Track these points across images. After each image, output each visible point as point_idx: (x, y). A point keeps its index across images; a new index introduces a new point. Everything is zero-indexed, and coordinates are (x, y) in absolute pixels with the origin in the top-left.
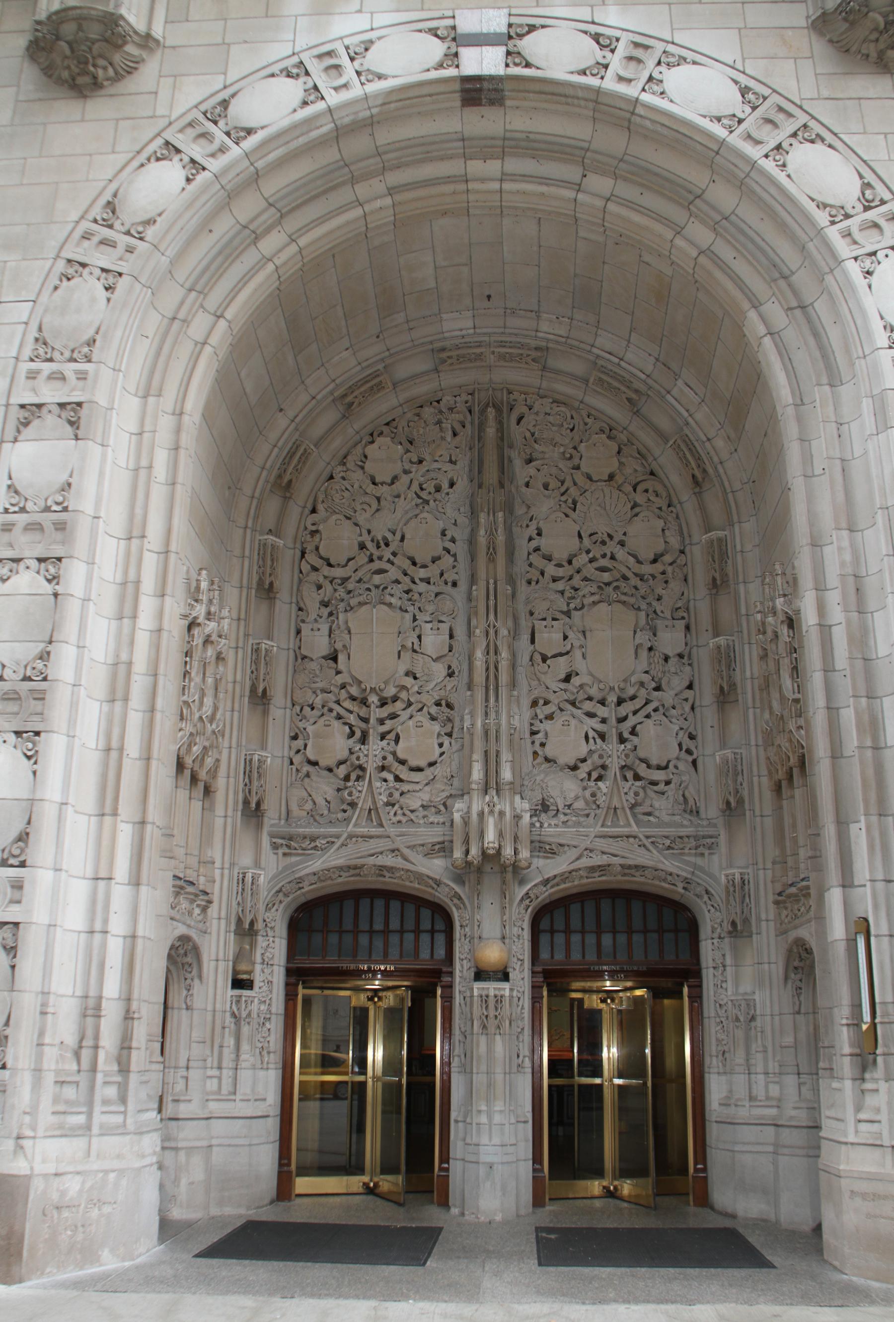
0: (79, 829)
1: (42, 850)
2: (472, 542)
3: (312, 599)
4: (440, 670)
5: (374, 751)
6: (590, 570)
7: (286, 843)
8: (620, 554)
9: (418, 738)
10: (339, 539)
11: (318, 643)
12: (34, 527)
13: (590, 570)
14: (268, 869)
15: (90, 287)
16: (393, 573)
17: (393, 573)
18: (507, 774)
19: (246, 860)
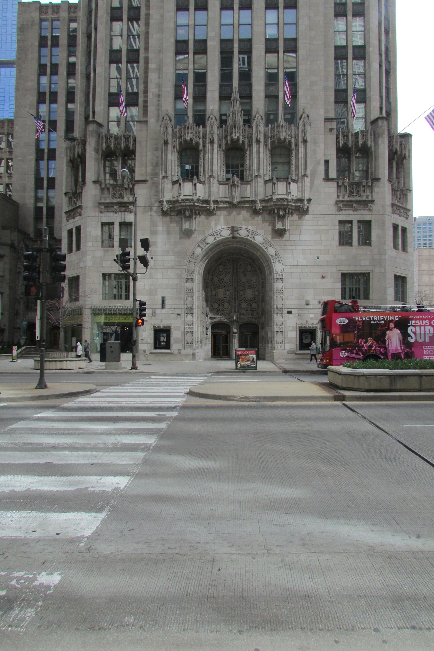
0: (197, 321)
1: (194, 325)
2: (232, 280)
3: (213, 288)
4: (228, 297)
5: (221, 307)
6: (247, 284)
7: (211, 318)
8: (251, 282)
9: (226, 305)
10: (216, 279)
11: (214, 293)
12: (190, 292)
13: (247, 284)
14: (209, 321)
15: (192, 264)
16: (223, 284)
17: (223, 284)
18: (237, 310)
19: (207, 320)
